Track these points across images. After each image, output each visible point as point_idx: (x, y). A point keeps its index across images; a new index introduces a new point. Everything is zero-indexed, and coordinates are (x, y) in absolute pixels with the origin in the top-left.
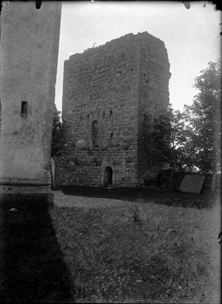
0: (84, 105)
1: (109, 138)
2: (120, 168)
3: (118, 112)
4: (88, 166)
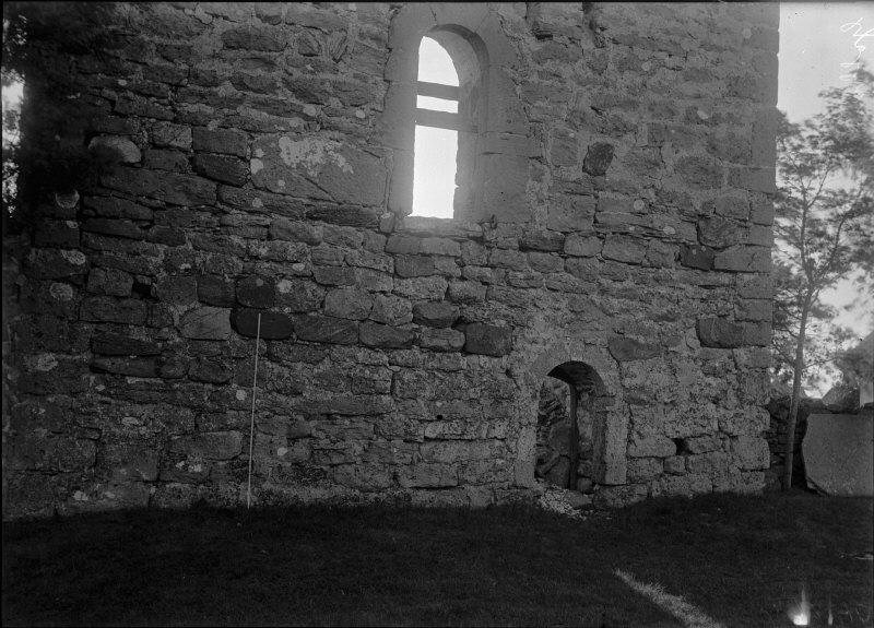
1: (575, 173)
4: (385, 347)
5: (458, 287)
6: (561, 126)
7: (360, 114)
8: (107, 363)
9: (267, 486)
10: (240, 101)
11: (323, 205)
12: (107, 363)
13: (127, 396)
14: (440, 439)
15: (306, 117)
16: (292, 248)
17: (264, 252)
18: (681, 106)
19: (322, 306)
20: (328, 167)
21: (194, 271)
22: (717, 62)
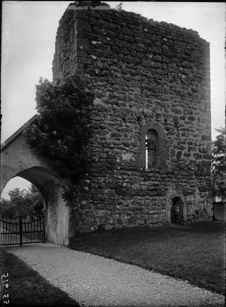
0: (131, 100)
1: (175, 158)
2: (192, 199)
3: (186, 126)
4: (143, 196)
5: (155, 183)
6: (172, 148)
7: (136, 149)
8: (95, 202)
9: (124, 224)
10: (114, 148)
11: (130, 168)
12: (95, 202)
13: (99, 209)
14: (154, 214)
15: (126, 150)
16: (125, 177)
17: (121, 178)
18: (194, 142)
20: (131, 160)
21: (109, 182)
22: (200, 133)
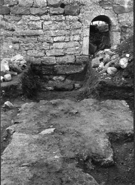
4: (39, 15)
19: (18, 4)
